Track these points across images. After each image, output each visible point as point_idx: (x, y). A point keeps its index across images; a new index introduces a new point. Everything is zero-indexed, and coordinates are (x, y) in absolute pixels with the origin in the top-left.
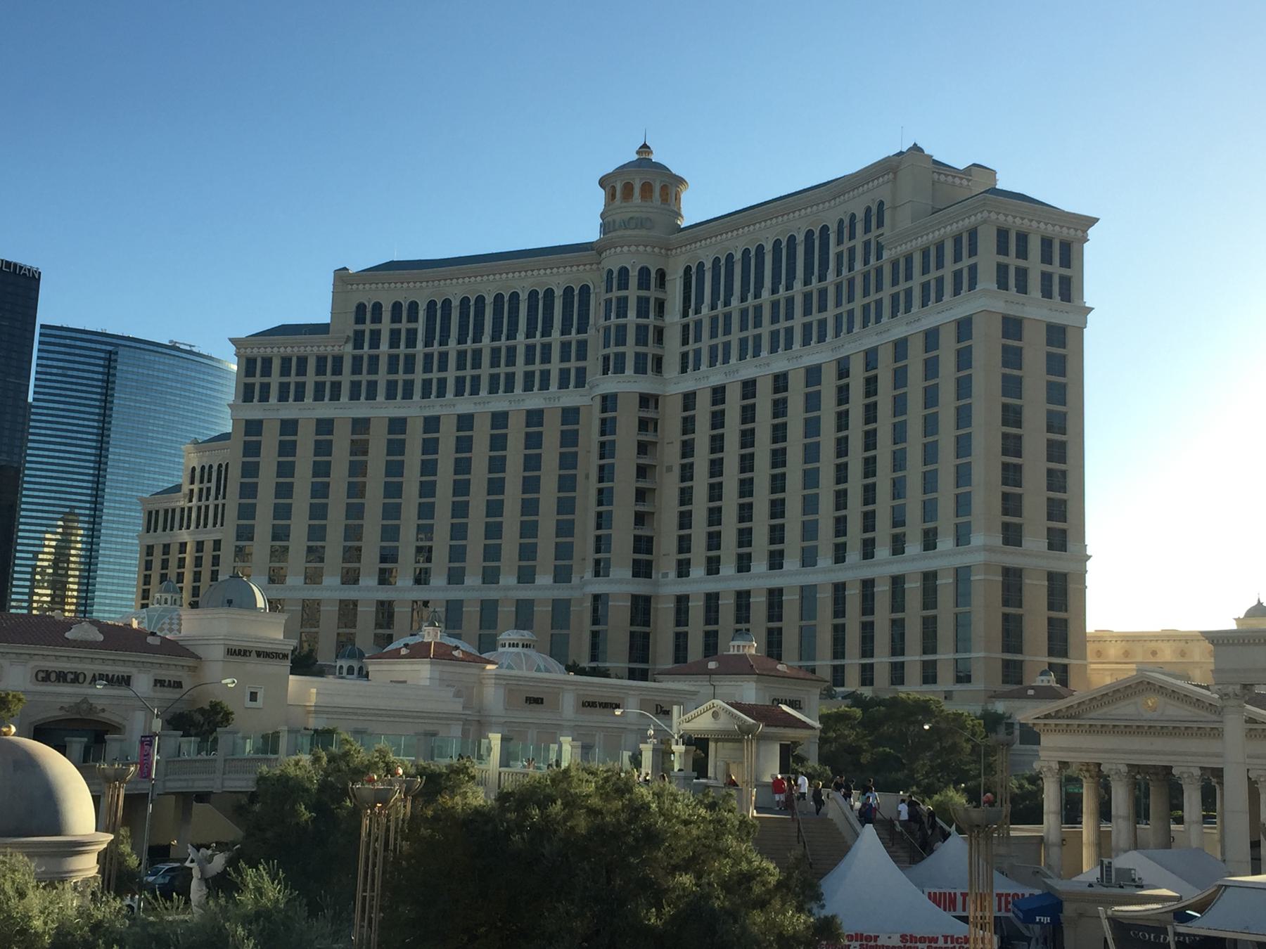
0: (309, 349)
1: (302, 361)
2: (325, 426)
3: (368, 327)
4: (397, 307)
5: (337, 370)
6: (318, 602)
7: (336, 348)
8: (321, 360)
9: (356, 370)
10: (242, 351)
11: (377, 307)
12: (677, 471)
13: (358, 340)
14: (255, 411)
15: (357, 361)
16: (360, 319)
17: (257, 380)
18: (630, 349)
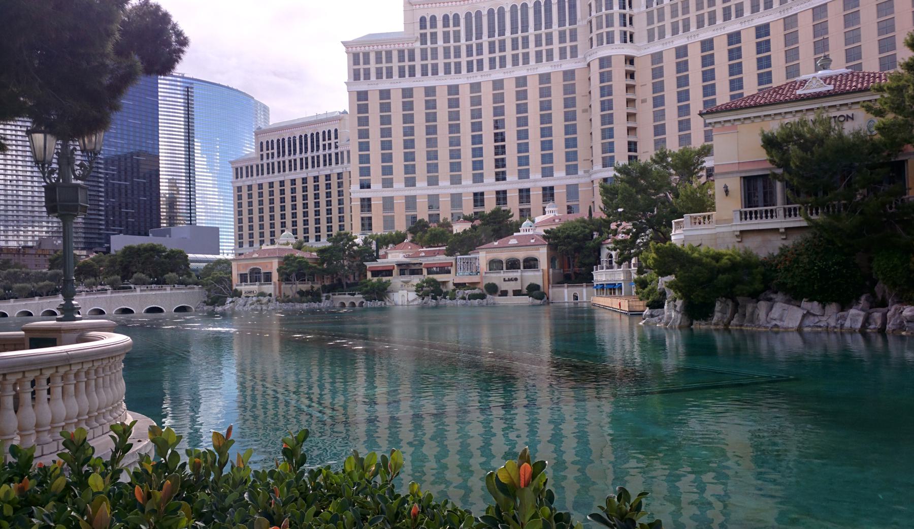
0: (392, 46)
1: (389, 54)
2: (408, 93)
3: (428, 31)
4: (446, 18)
5: (412, 58)
6: (414, 197)
7: (410, 45)
8: (401, 53)
9: (424, 57)
10: (350, 49)
11: (433, 19)
12: (650, 102)
13: (423, 38)
14: (362, 86)
15: (424, 53)
16: (423, 25)
17: (362, 66)
18: (617, 29)
